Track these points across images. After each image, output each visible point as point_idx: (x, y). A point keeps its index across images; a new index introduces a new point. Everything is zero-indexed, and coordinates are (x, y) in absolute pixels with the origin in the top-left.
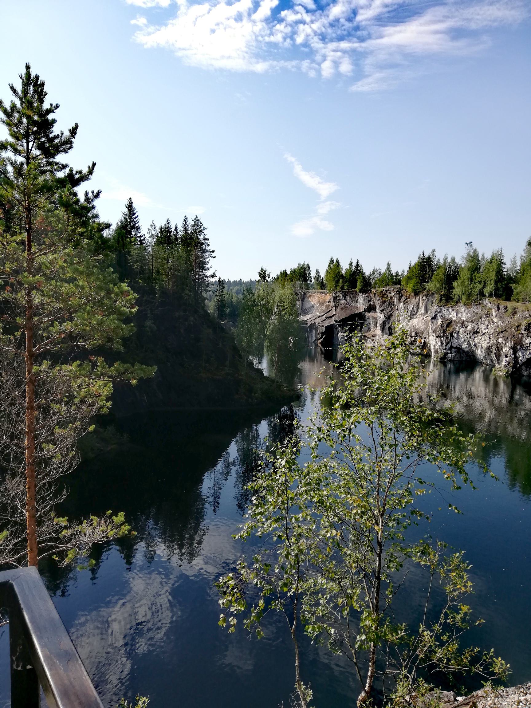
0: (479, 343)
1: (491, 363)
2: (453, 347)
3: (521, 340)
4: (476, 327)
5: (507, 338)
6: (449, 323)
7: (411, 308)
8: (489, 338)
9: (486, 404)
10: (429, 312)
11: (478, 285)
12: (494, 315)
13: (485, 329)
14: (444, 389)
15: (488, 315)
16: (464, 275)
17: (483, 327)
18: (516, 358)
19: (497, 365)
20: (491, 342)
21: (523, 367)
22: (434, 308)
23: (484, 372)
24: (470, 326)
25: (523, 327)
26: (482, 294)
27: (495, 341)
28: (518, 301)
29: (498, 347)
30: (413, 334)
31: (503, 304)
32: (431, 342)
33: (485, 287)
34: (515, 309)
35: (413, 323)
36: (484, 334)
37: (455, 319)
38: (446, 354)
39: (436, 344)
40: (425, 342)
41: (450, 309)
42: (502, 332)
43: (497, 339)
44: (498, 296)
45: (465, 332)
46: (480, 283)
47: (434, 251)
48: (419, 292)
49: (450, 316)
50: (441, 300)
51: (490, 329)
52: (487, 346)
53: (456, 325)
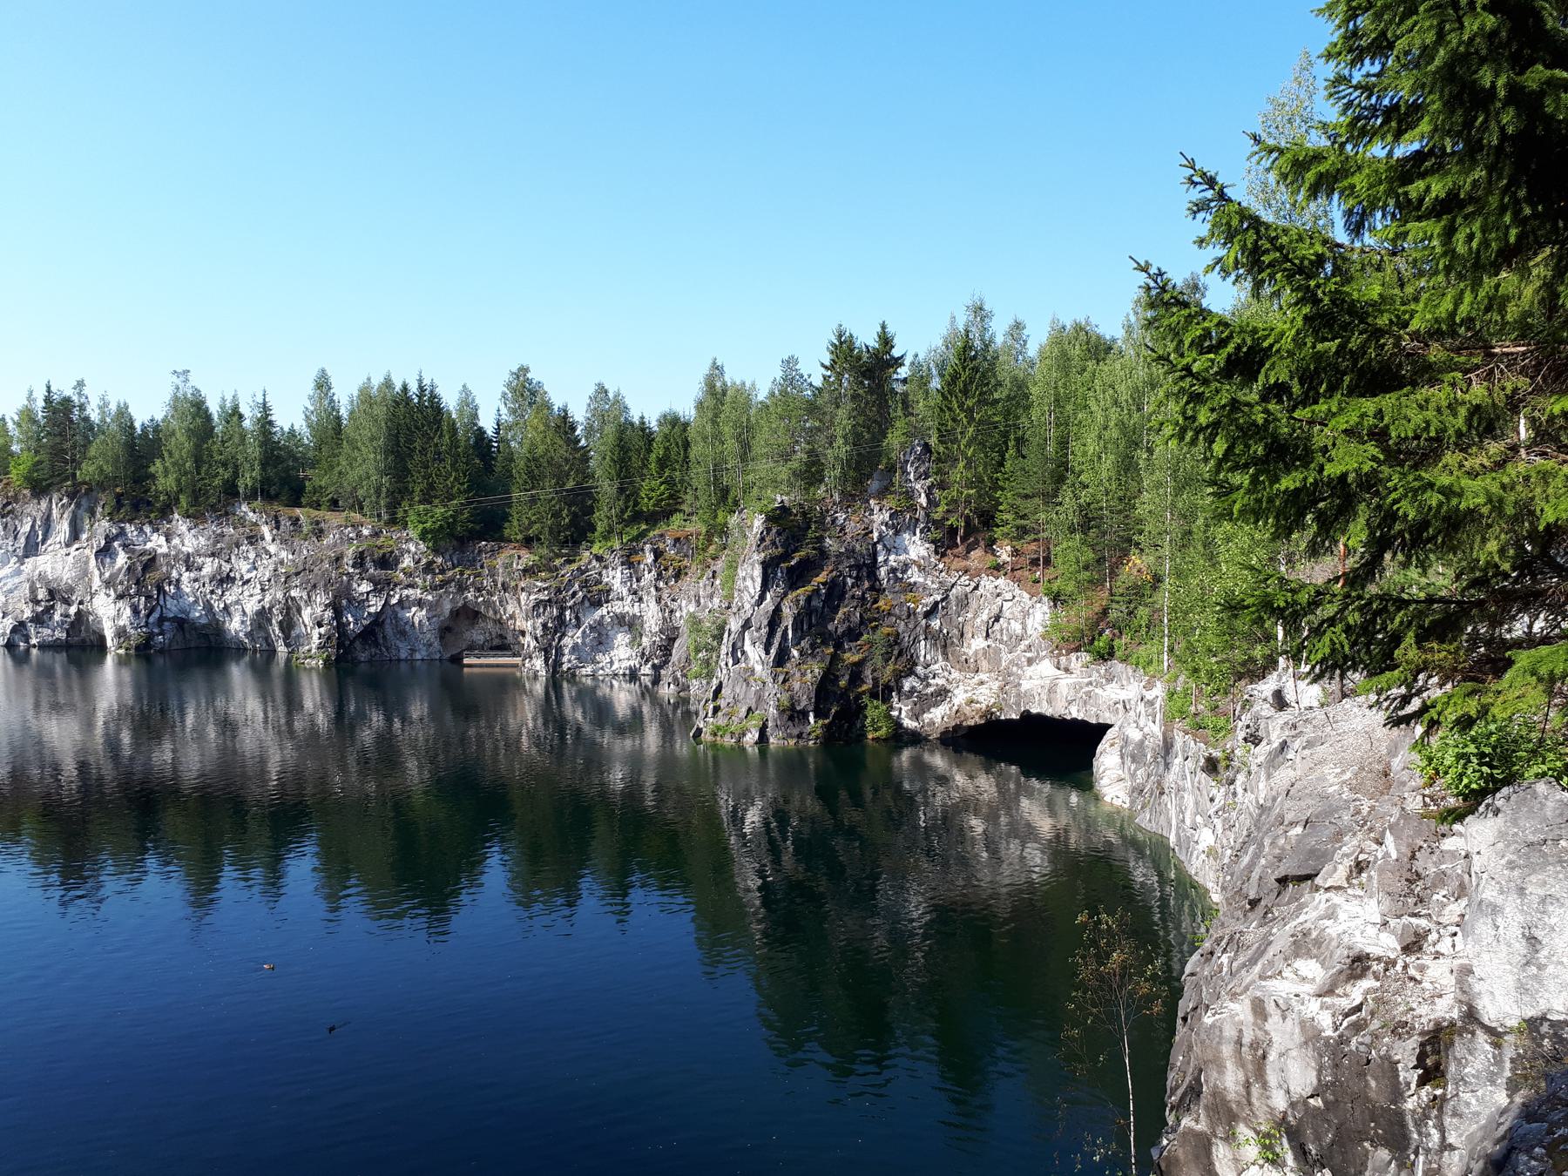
0: (237, 602)
1: (265, 646)
2: (168, 619)
3: (349, 587)
4: (226, 567)
5: (315, 586)
6: (151, 562)
7: (27, 528)
8: (263, 590)
9: (270, 738)
10: (84, 536)
11: (221, 470)
12: (268, 537)
13: (249, 571)
14: (150, 717)
15: (254, 539)
16: (180, 445)
17: (244, 567)
18: (341, 627)
19: (282, 649)
20: (268, 598)
21: (358, 644)
22: (104, 526)
23: (253, 666)
24: (209, 567)
25: (348, 560)
26: (231, 491)
27: (280, 595)
28: (317, 506)
29: (288, 608)
30: (42, 594)
31: (285, 513)
32: (101, 612)
33: (236, 475)
34: (318, 523)
35: (35, 568)
36: (248, 581)
37: (164, 550)
38: (150, 637)
39: (119, 615)
40: (79, 613)
41: (147, 529)
42: (297, 574)
43: (288, 589)
44: (269, 497)
45: (196, 580)
46: (225, 465)
47: (80, 384)
48: (49, 485)
49: (149, 546)
50: (119, 505)
51: (261, 569)
52: (257, 607)
53: (168, 564)
